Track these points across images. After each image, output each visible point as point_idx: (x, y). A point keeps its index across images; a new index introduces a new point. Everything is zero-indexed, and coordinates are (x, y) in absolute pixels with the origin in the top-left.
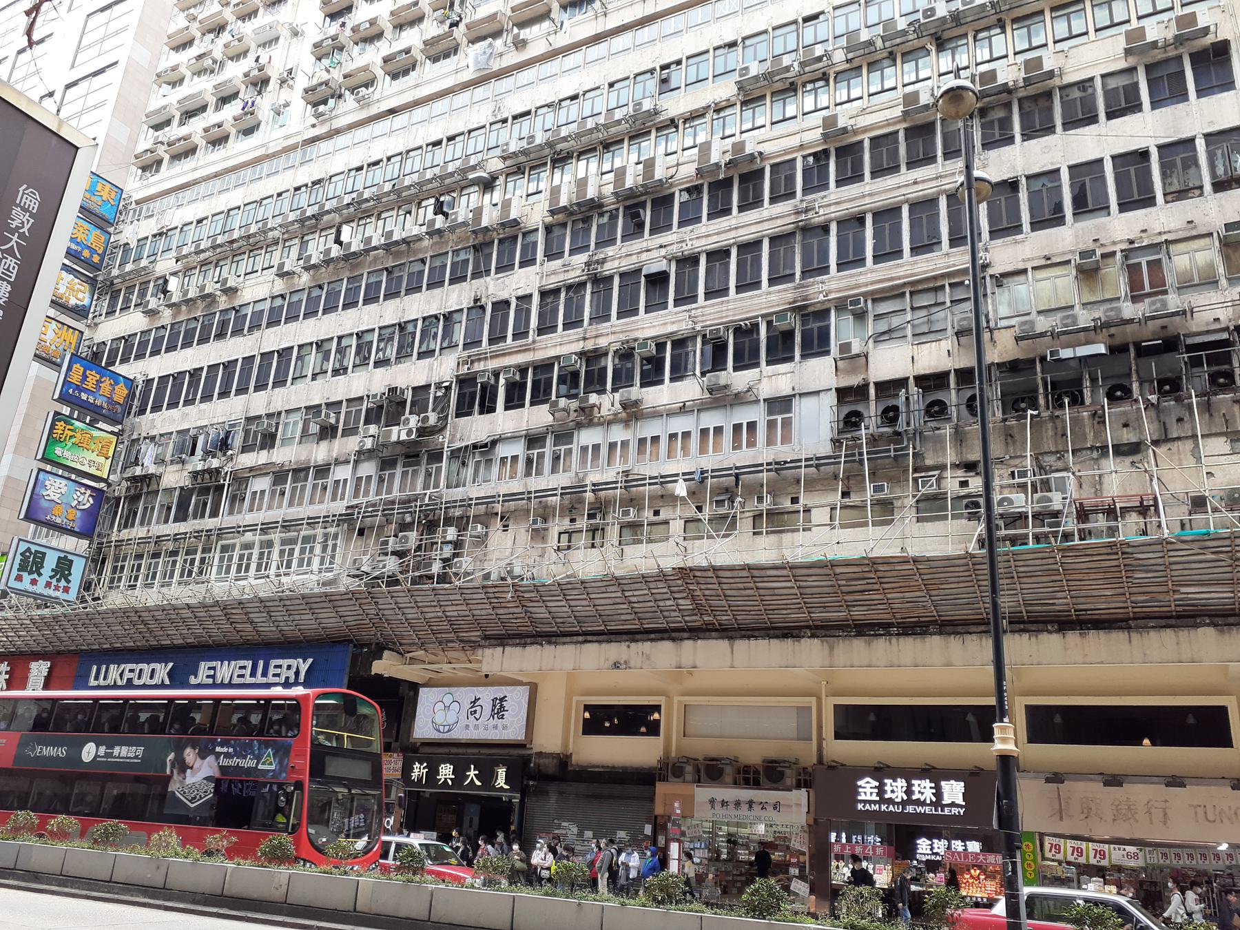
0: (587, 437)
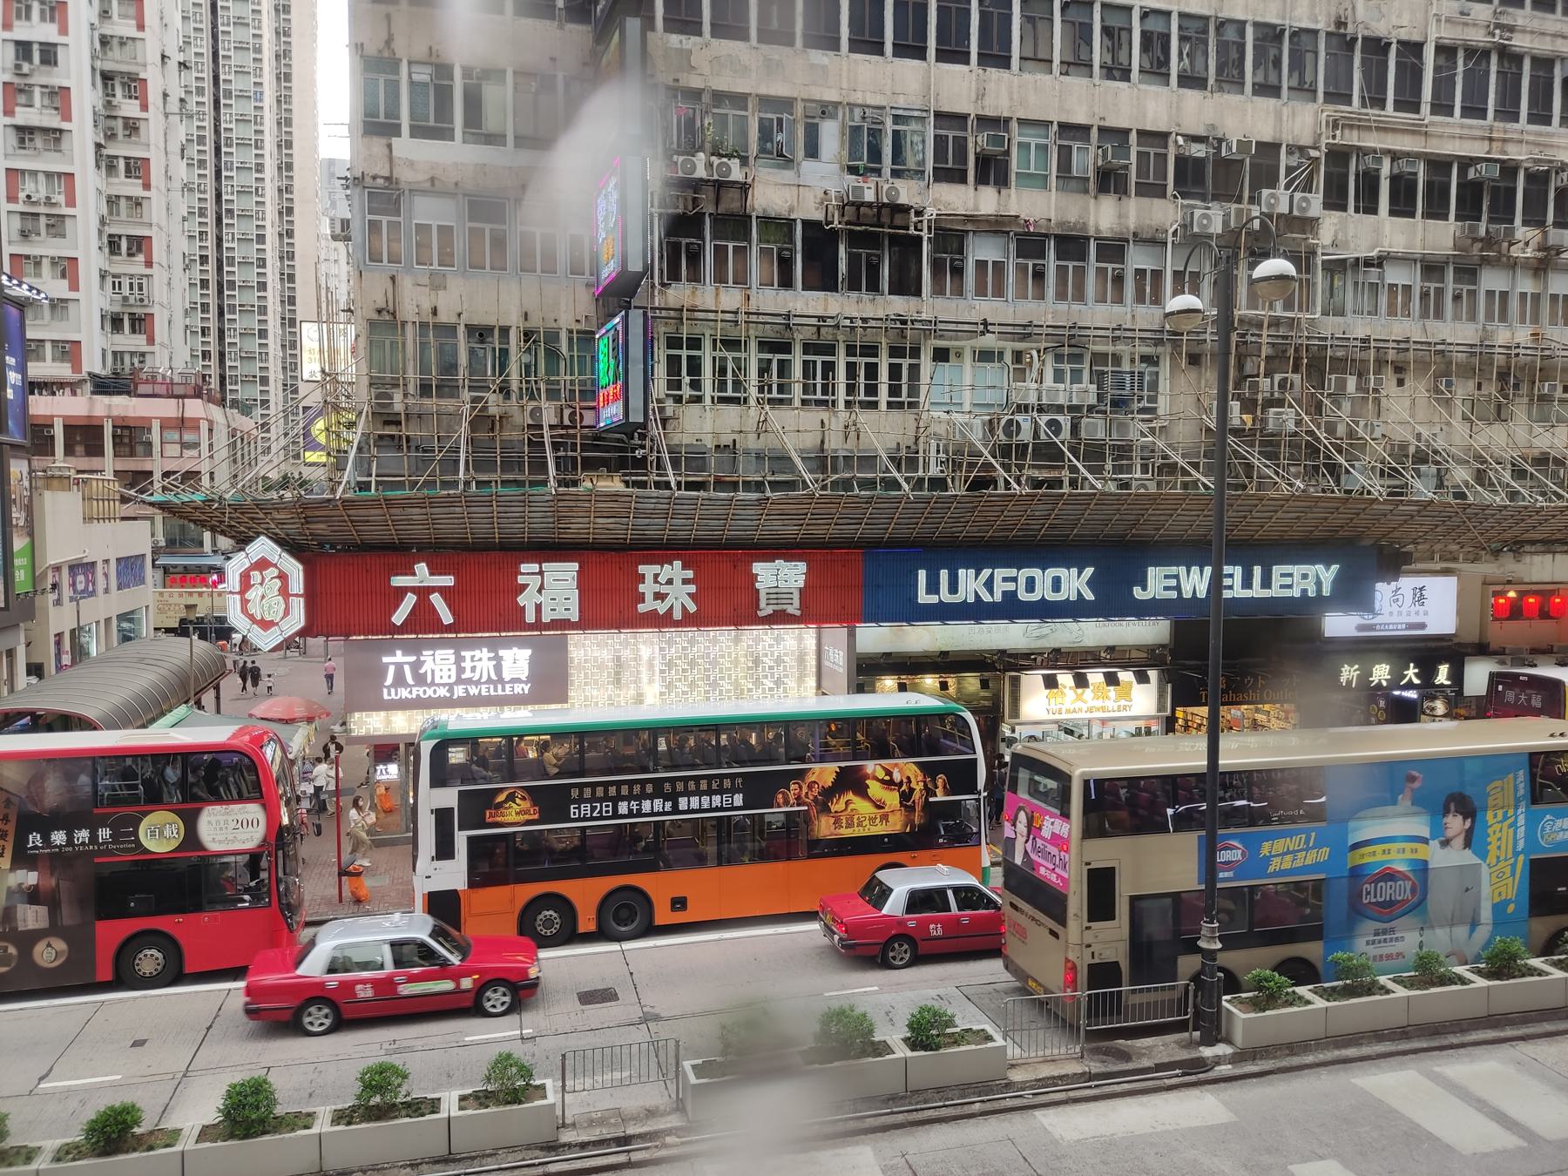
0: (1491, 280)
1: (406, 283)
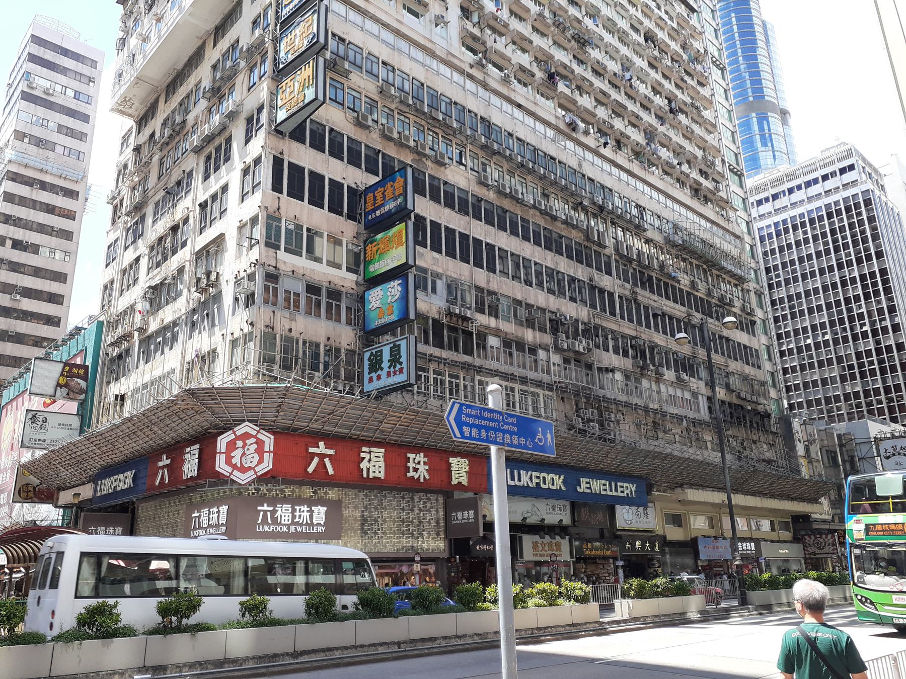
1: (278, 314)
